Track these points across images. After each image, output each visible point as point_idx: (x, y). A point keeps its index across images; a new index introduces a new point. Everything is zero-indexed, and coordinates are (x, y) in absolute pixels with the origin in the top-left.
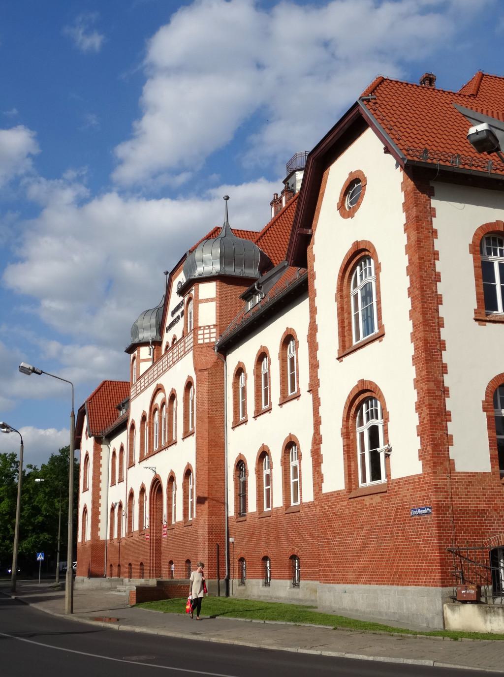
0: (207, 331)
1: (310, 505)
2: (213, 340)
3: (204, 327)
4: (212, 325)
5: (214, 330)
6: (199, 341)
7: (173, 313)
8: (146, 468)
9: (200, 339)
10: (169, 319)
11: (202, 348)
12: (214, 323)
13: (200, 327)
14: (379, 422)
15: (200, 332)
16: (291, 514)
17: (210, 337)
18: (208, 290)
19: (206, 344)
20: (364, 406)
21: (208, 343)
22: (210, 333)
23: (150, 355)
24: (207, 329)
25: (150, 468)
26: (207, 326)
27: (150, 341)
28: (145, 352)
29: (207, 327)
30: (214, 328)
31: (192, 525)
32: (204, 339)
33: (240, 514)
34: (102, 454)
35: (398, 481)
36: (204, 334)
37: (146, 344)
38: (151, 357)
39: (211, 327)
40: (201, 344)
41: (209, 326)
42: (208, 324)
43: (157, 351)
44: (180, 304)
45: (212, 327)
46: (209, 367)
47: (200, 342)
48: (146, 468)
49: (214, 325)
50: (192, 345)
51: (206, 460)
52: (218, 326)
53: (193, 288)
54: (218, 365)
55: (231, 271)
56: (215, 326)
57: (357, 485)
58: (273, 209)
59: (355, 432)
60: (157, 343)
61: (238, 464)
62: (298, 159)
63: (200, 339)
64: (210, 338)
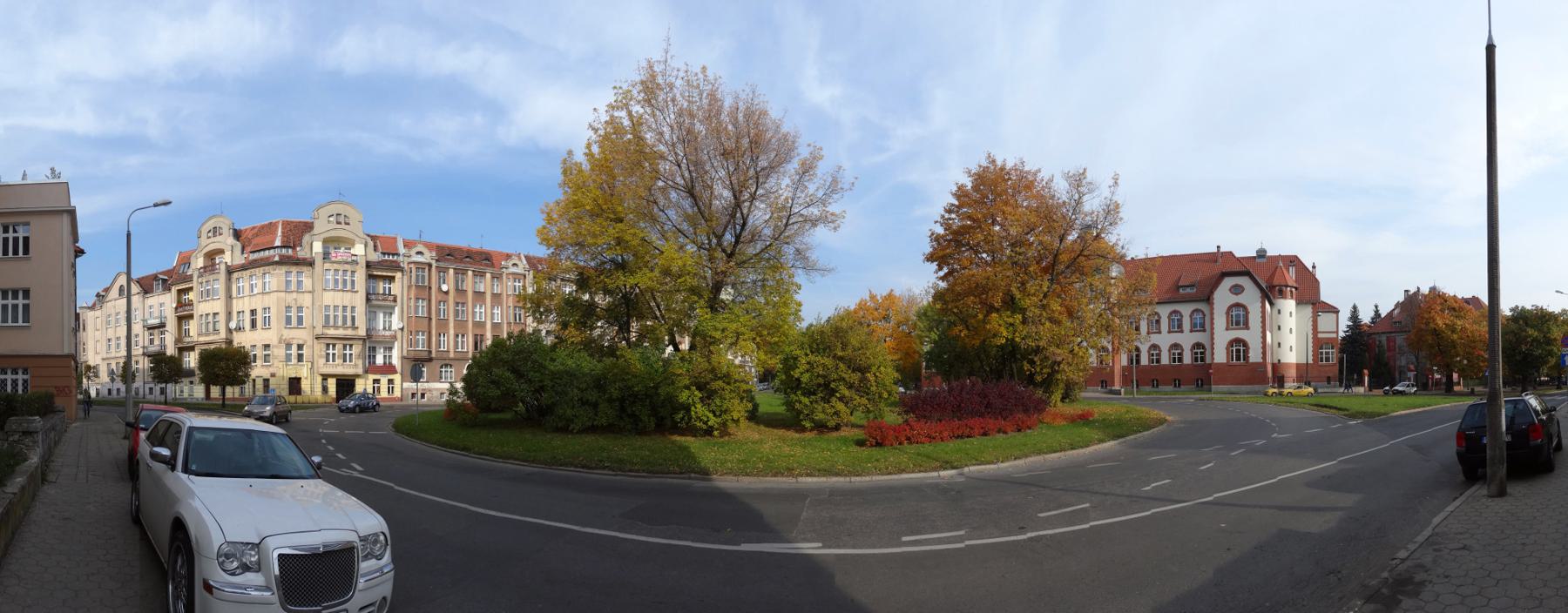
1: (1188, 365)
14: (1242, 348)
35: (1252, 363)
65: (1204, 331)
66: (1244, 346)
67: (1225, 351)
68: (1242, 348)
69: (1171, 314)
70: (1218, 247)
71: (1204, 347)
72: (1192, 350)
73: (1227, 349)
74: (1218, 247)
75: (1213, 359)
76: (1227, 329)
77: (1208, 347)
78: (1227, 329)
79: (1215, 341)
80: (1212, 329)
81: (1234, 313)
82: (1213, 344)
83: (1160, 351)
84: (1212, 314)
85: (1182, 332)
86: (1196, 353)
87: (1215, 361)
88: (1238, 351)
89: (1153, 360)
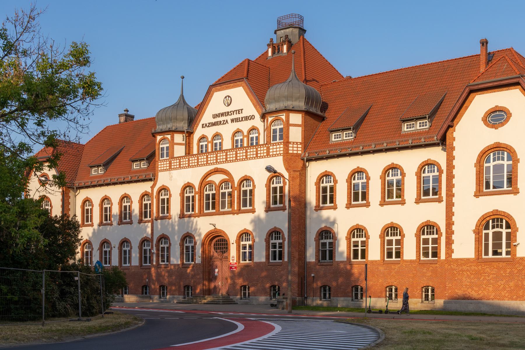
0: (296, 146)
1: (411, 261)
2: (300, 152)
3: (294, 142)
4: (299, 142)
5: (300, 146)
6: (289, 151)
7: (215, 116)
8: (210, 224)
9: (290, 150)
10: (207, 117)
11: (291, 156)
12: (301, 141)
13: (291, 142)
15: (290, 145)
16: (389, 265)
17: (296, 149)
18: (296, 118)
19: (295, 153)
20: (491, 221)
21: (296, 153)
22: (297, 147)
23: (183, 141)
24: (295, 144)
25: (212, 224)
26: (295, 142)
27: (185, 131)
28: (179, 138)
29: (296, 143)
30: (300, 144)
31: (281, 265)
32: (293, 150)
33: (319, 261)
34: (70, 200)
36: (293, 147)
37: (182, 132)
38: (184, 142)
39: (298, 143)
40: (291, 153)
41: (297, 143)
42: (293, 141)
43: (188, 139)
44: (228, 112)
45: (299, 144)
46: (300, 170)
47: (290, 152)
48: (210, 224)
49: (300, 143)
50: (282, 152)
51: (297, 227)
52: (303, 144)
53: (284, 114)
54: (303, 169)
55: (313, 110)
56: (301, 143)
57: (482, 256)
58: (270, 50)
59: (482, 232)
60: (190, 134)
61: (321, 233)
62: (293, 18)
63: (290, 150)
64: (297, 150)
65: (440, 201)
66: (508, 226)
67: (473, 236)
68: (504, 231)
69: (386, 171)
70: (484, 43)
71: (438, 231)
72: (418, 236)
73: (477, 232)
74: (484, 43)
75: (450, 251)
76: (476, 195)
77: (443, 230)
78: (476, 195)
79: (454, 218)
80: (450, 195)
81: (492, 164)
82: (449, 224)
83: (367, 237)
84: (450, 167)
85: (403, 203)
86: (426, 241)
87: (454, 256)
88: (497, 236)
89: (356, 252)
